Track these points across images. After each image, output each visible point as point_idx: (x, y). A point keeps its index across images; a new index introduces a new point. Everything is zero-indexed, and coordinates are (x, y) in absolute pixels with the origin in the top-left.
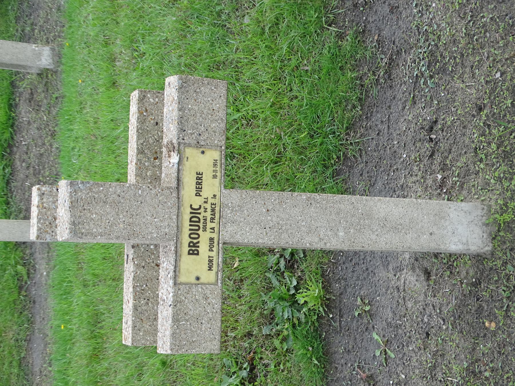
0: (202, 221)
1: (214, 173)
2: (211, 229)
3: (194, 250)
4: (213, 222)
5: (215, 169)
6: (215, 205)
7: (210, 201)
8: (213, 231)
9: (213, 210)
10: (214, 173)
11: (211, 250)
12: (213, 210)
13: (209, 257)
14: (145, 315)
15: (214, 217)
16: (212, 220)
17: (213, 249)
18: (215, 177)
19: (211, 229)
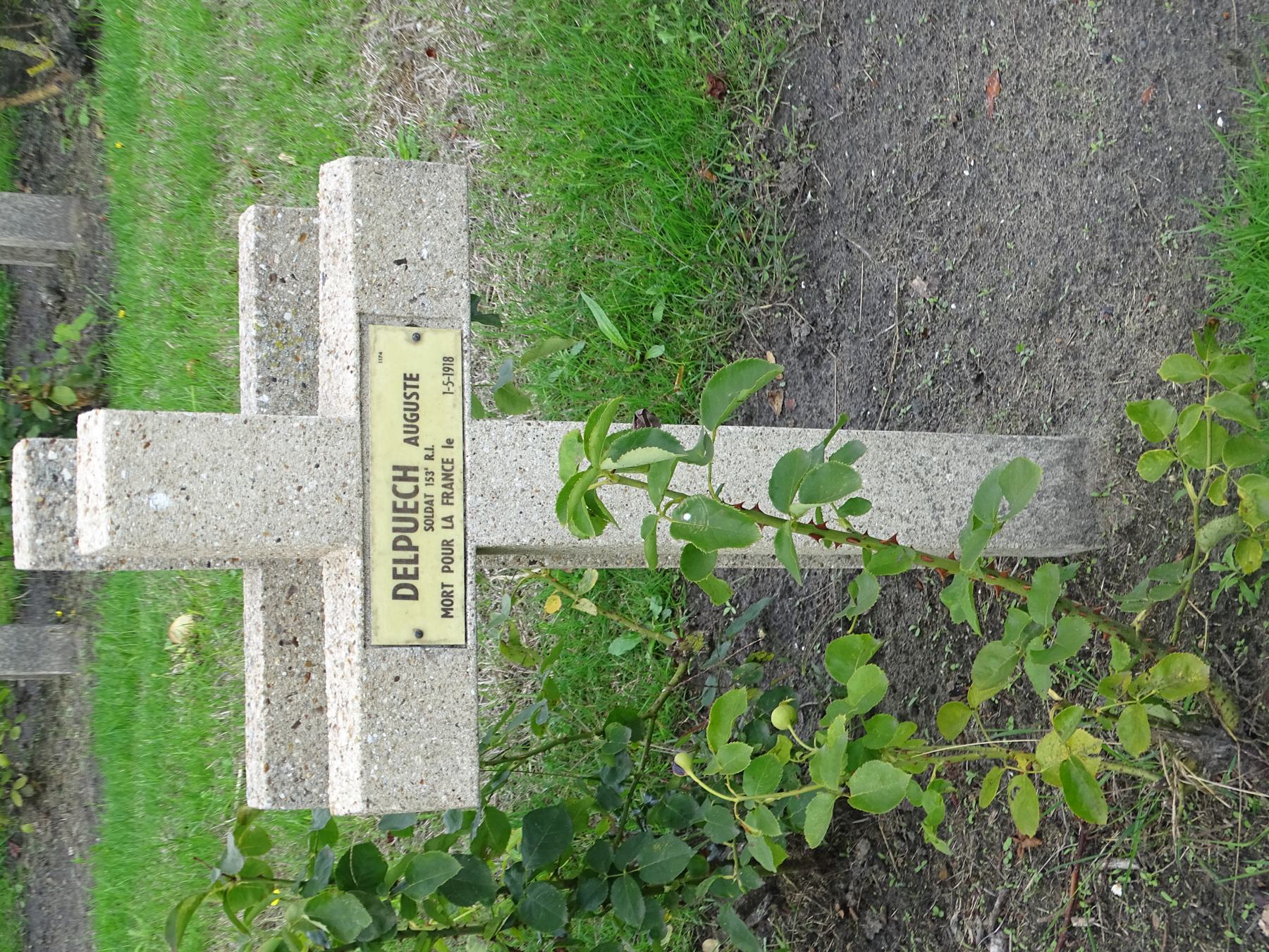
2: (444, 519)
4: (448, 503)
6: (452, 462)
7: (440, 454)
8: (449, 524)
9: (447, 476)
11: (447, 569)
12: (447, 476)
13: (443, 586)
16: (447, 498)
19: (444, 519)
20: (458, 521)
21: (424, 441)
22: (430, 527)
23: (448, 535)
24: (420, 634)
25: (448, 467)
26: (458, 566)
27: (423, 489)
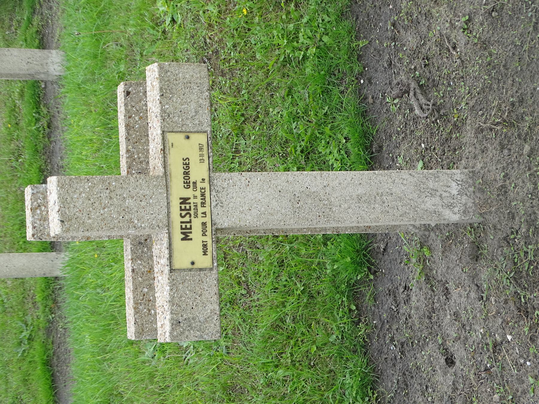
0: (192, 208)
1: (201, 158)
2: (202, 213)
3: (186, 237)
5: (201, 153)
7: (199, 185)
9: (203, 195)
10: (201, 158)
11: (204, 234)
12: (203, 195)
13: (203, 242)
14: (146, 302)
15: (204, 201)
16: (203, 204)
17: (206, 233)
18: (202, 161)
19: (202, 213)
20: (208, 214)
21: (192, 180)
22: (196, 216)
23: (204, 220)
24: (193, 263)
25: (203, 191)
26: (209, 233)
27: (192, 201)
